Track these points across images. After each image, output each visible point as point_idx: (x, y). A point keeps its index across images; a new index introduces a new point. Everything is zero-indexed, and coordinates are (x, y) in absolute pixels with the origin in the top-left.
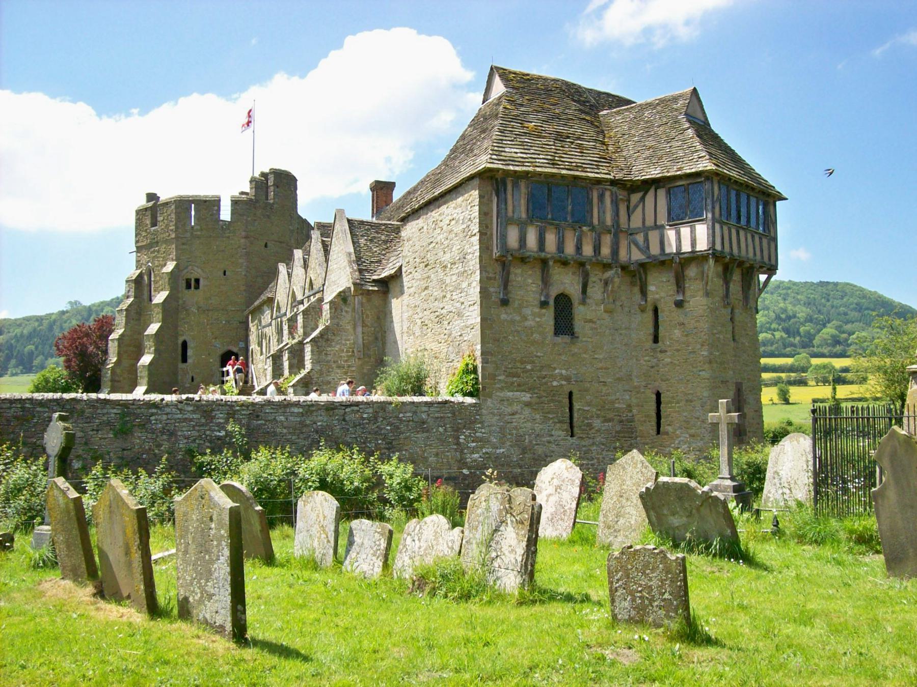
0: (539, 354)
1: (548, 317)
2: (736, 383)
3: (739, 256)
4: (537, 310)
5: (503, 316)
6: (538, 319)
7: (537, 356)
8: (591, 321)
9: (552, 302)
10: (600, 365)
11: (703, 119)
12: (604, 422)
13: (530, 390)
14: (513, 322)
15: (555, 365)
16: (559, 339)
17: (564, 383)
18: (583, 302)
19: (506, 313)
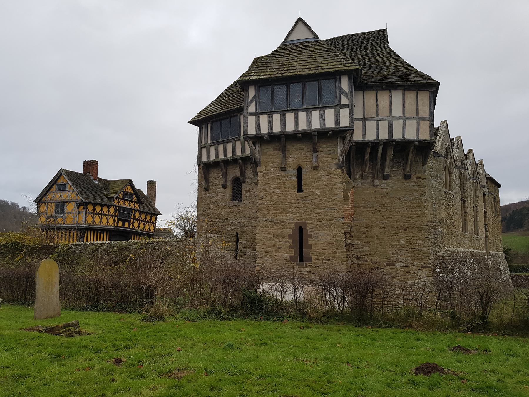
0: (222, 213)
1: (228, 192)
2: (296, 223)
3: (284, 132)
4: (222, 189)
5: (208, 195)
6: (222, 194)
7: (221, 215)
8: (249, 191)
9: (229, 184)
10: (253, 216)
11: (312, 36)
12: (252, 250)
13: (218, 233)
14: (212, 198)
15: (230, 219)
16: (232, 204)
17: (233, 228)
18: (244, 182)
19: (209, 193)
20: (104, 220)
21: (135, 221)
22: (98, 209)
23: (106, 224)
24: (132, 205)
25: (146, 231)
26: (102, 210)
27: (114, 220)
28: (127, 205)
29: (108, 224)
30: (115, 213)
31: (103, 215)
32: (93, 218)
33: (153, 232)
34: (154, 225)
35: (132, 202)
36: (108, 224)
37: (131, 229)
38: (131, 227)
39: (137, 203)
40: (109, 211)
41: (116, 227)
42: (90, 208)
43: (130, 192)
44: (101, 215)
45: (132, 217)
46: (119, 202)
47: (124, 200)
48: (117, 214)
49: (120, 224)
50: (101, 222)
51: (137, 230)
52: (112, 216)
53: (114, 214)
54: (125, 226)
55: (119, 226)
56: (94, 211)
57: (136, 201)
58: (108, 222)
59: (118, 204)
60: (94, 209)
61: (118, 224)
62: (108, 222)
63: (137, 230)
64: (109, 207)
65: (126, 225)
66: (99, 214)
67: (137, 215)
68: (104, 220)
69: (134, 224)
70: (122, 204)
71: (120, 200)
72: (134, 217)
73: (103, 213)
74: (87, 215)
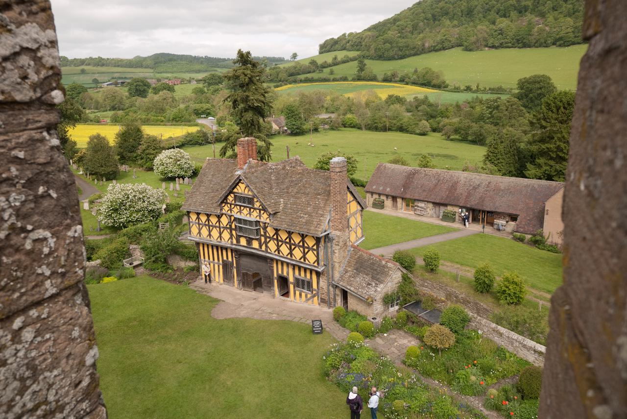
20: (215, 233)
21: (268, 240)
22: (203, 218)
23: (219, 239)
24: (255, 213)
25: (297, 261)
26: (208, 220)
27: (232, 235)
28: (245, 215)
29: (221, 240)
30: (231, 226)
31: (212, 226)
32: (200, 230)
33: (316, 264)
34: (315, 252)
35: (255, 209)
36: (221, 240)
37: (263, 251)
38: (264, 248)
39: (265, 210)
40: (219, 221)
41: (235, 245)
42: (194, 217)
43: (246, 192)
44: (210, 227)
45: (262, 233)
46: (231, 210)
47: (240, 206)
48: (233, 227)
49: (243, 242)
50: (210, 235)
51: (276, 255)
52: (225, 228)
53: (228, 226)
54: (253, 246)
55: (241, 244)
56: (199, 221)
57: (261, 207)
58: (220, 237)
59: (231, 212)
60: (198, 218)
61: (238, 241)
62: (220, 237)
63: (276, 255)
64: (219, 217)
65: (255, 244)
66: (206, 225)
67: (271, 232)
68: (215, 233)
69: (269, 245)
70: (235, 212)
71: (233, 206)
72: (265, 233)
73: (211, 224)
74: (191, 224)
